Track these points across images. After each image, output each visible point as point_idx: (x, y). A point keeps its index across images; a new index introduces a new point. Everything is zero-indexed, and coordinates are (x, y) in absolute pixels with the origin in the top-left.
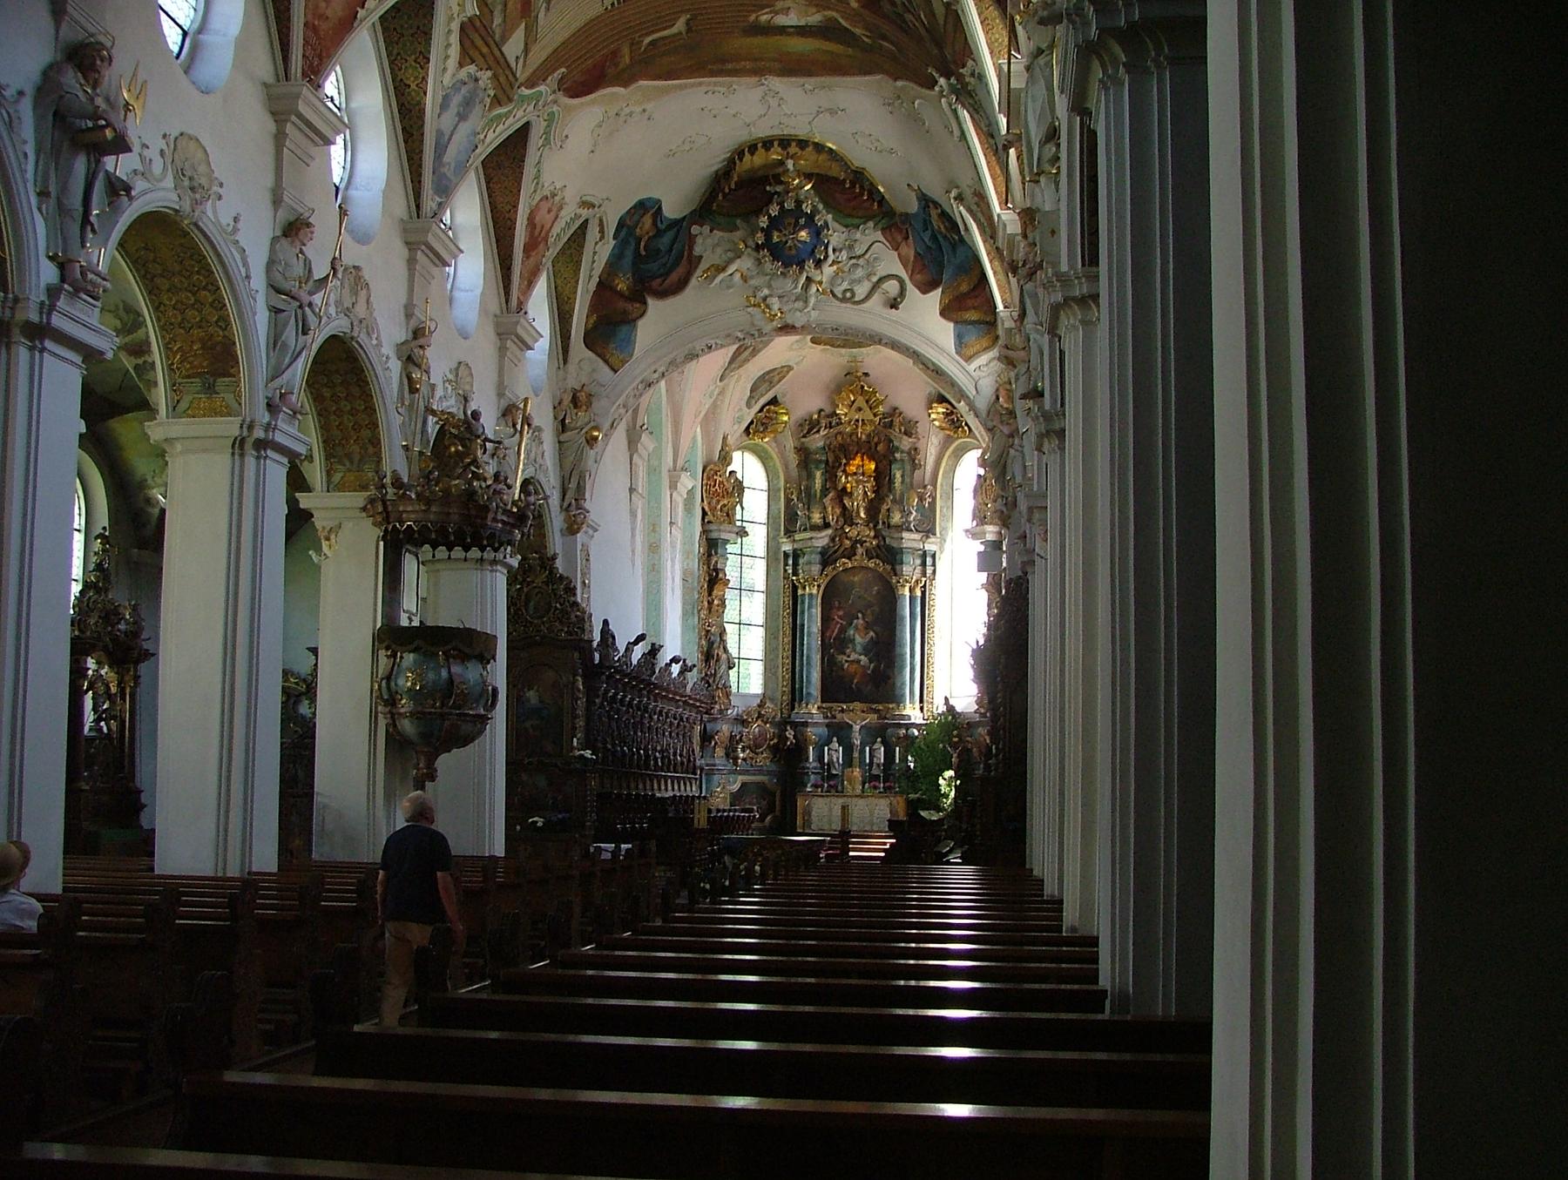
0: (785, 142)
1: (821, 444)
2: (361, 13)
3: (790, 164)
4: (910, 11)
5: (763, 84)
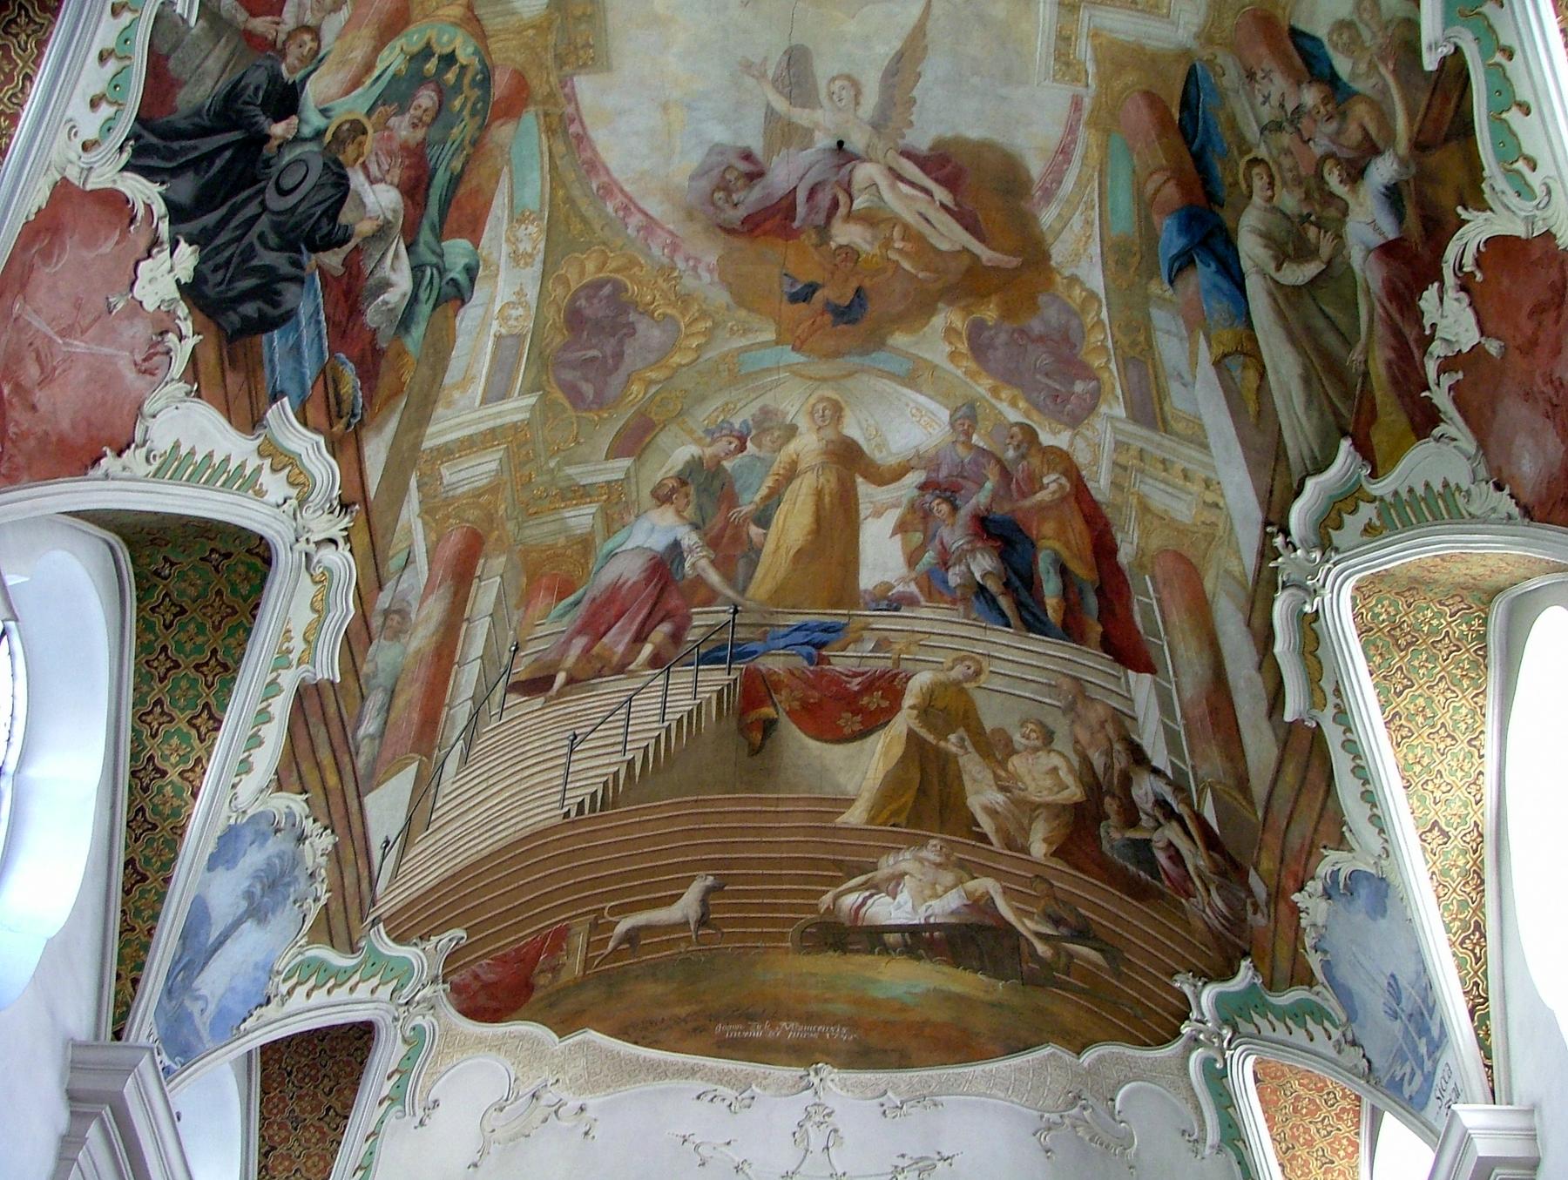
4: (1170, 814)
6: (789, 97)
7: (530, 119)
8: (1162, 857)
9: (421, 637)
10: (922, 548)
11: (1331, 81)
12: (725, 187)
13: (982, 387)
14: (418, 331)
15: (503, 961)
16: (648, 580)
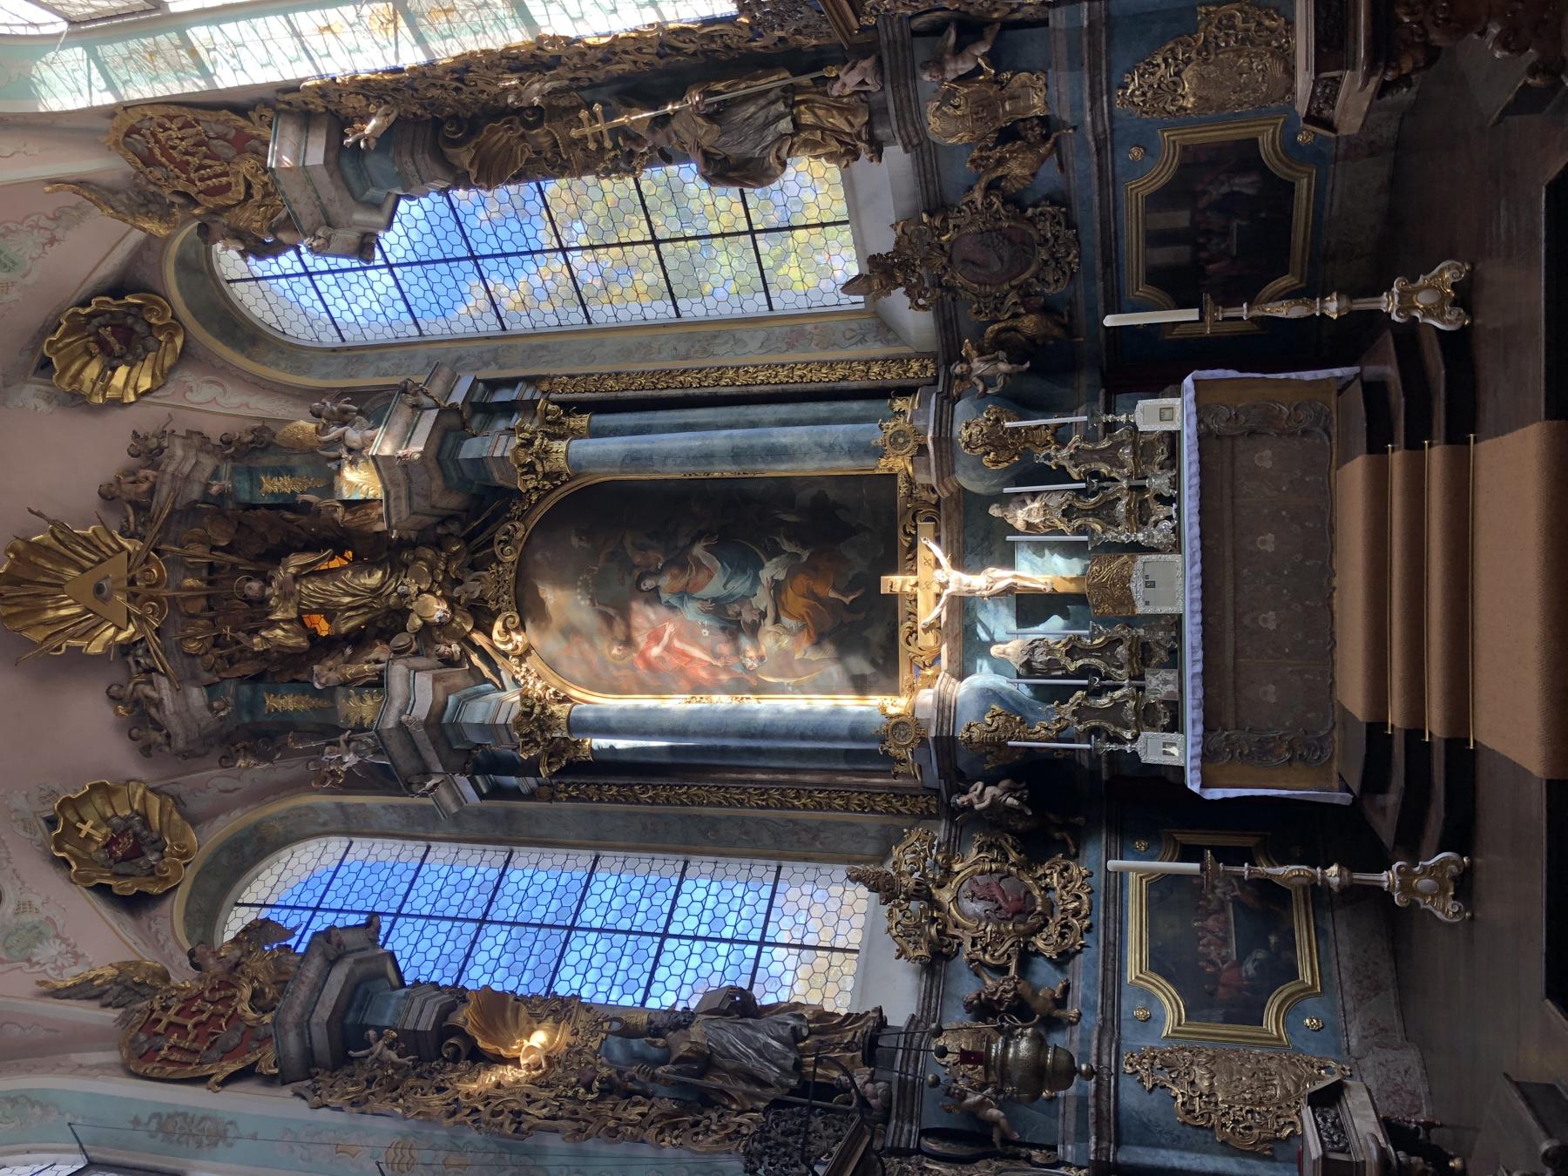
1: (196, 696)
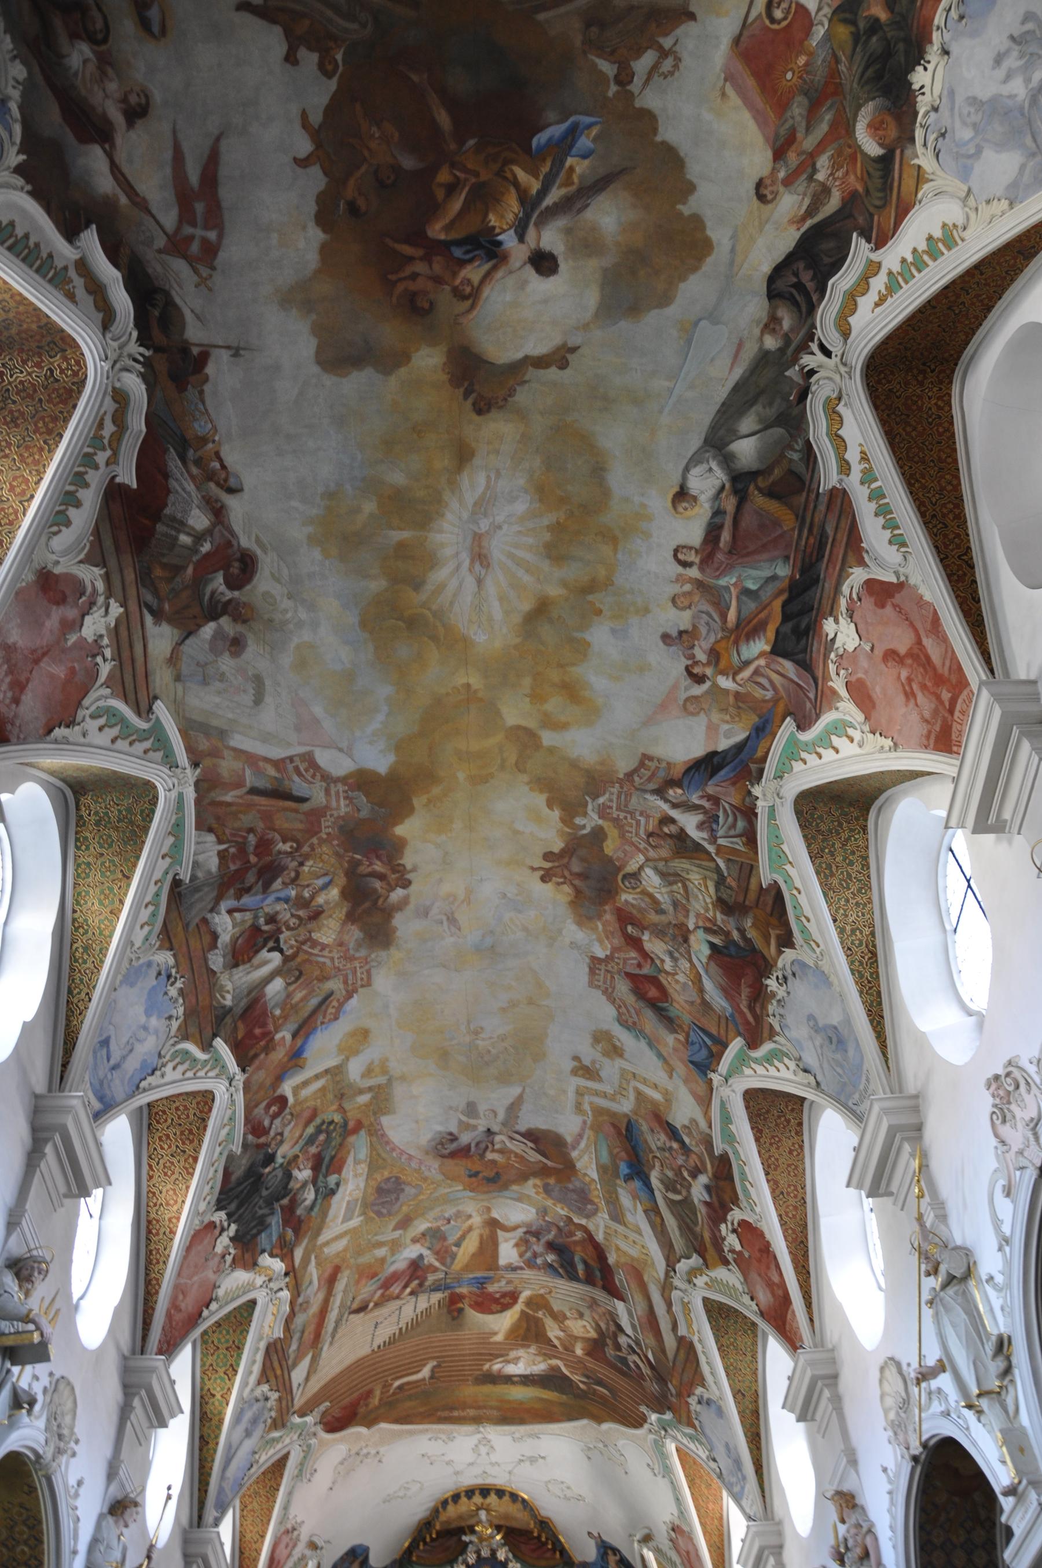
0: (485, 1491)
2: (205, 1313)
3: (483, 1515)
4: (634, 1352)
5: (479, 1432)
6: (468, 1116)
7: (363, 1133)
8: (632, 1365)
9: (314, 1309)
10: (526, 1252)
11: (682, 1143)
12: (442, 1144)
13: (549, 1203)
14: (316, 1210)
15: (345, 1408)
16: (409, 1267)
